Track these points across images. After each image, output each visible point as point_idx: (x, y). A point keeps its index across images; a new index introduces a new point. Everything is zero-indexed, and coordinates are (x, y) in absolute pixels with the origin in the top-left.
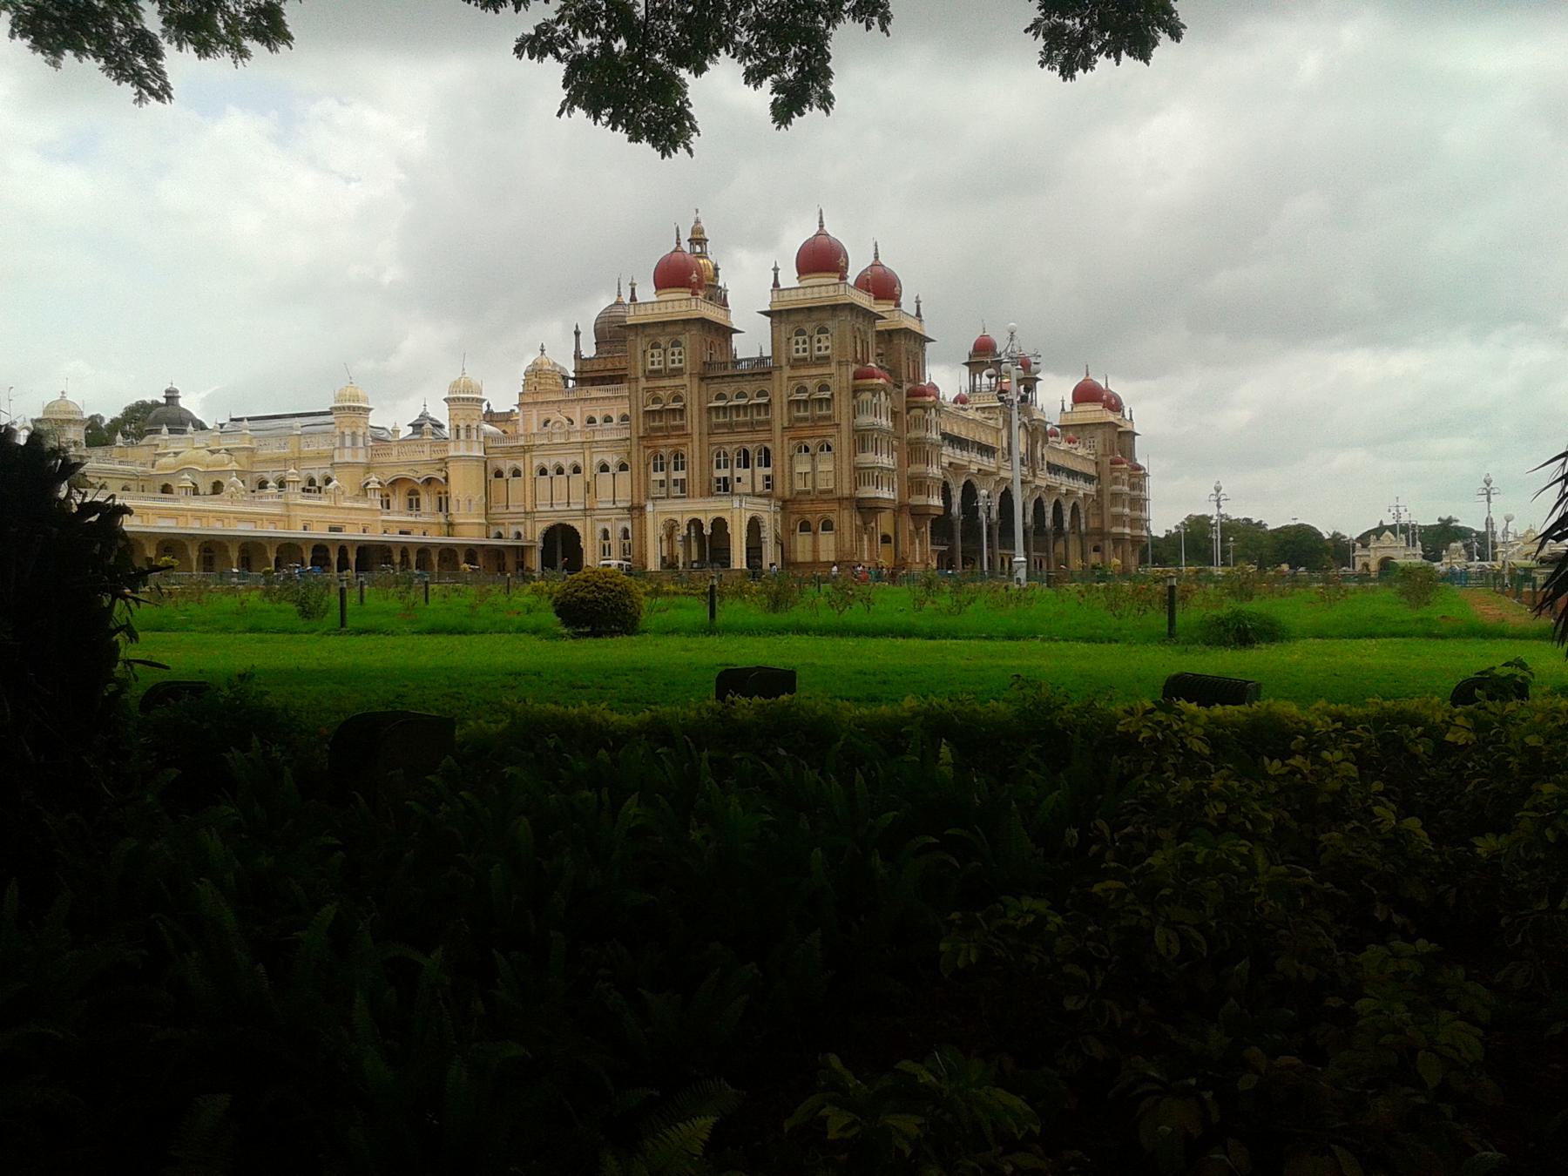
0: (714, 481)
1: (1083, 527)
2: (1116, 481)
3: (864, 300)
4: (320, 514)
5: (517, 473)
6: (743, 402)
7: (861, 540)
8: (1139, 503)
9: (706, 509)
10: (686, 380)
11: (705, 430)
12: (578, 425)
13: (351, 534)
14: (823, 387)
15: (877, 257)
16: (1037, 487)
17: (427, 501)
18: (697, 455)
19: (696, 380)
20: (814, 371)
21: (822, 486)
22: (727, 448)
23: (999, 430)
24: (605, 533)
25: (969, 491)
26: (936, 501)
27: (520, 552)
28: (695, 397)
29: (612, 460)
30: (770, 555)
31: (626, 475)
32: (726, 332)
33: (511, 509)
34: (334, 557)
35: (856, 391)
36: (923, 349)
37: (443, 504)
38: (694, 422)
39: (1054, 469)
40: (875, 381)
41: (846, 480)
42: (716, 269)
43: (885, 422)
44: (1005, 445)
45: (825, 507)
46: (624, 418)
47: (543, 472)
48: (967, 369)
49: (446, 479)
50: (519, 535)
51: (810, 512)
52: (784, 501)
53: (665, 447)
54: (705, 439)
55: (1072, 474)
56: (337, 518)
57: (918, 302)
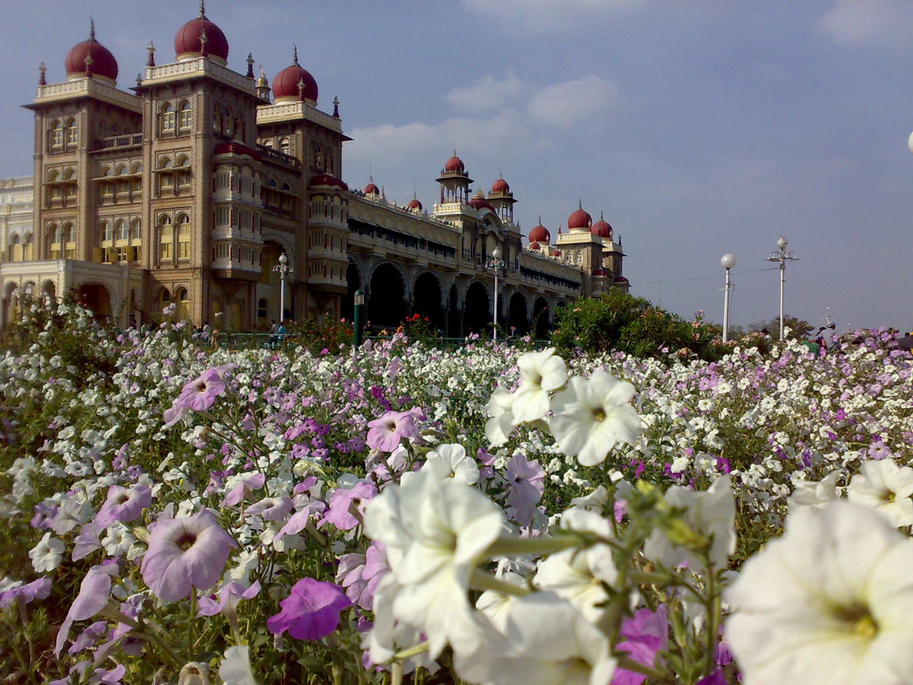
18: (83, 226)
19: (84, 156)
20: (177, 145)
22: (110, 220)
23: (458, 235)
28: (84, 170)
39: (526, 271)
41: (199, 249)
44: (467, 246)
45: (182, 276)
51: (167, 281)
53: (60, 217)
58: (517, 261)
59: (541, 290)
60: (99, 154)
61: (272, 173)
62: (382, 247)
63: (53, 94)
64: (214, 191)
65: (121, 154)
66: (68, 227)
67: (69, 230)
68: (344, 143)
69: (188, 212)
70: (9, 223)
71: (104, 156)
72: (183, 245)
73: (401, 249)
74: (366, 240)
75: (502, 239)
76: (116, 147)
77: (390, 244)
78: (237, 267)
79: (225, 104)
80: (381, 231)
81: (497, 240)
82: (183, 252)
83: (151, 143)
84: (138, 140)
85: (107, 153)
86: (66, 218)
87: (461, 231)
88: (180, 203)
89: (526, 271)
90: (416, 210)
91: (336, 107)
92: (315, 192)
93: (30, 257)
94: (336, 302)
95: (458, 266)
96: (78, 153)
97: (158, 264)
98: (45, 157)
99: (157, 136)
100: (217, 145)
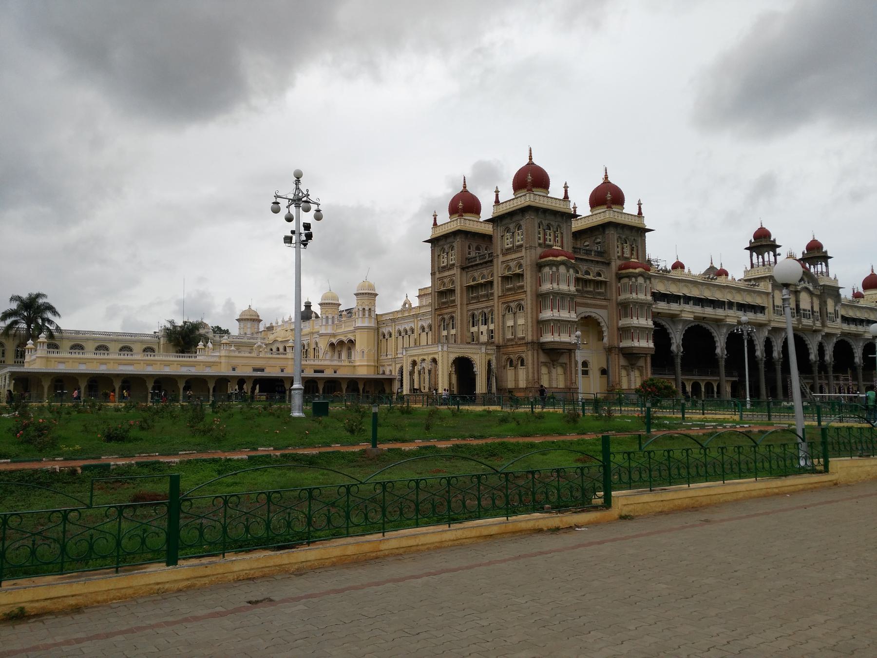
0: (469, 335)
4: (245, 361)
6: (482, 281)
11: (465, 302)
15: (606, 177)
16: (828, 336)
18: (459, 318)
20: (514, 256)
21: (520, 335)
22: (476, 312)
23: (768, 294)
29: (426, 325)
33: (389, 357)
35: (540, 267)
38: (457, 297)
39: (845, 319)
40: (551, 258)
41: (530, 329)
48: (748, 252)
52: (498, 347)
54: (465, 306)
56: (259, 363)
57: (640, 204)
60: (468, 267)
61: (584, 267)
62: (689, 312)
63: (440, 232)
65: (480, 267)
66: (452, 318)
68: (647, 234)
69: (523, 302)
71: (470, 269)
73: (709, 312)
74: (674, 307)
75: (819, 293)
77: (698, 310)
78: (557, 339)
79: (547, 222)
80: (687, 299)
81: (811, 293)
84: (491, 255)
85: (472, 266)
87: (770, 290)
88: (516, 297)
89: (845, 319)
91: (640, 209)
93: (430, 343)
94: (646, 360)
95: (770, 321)
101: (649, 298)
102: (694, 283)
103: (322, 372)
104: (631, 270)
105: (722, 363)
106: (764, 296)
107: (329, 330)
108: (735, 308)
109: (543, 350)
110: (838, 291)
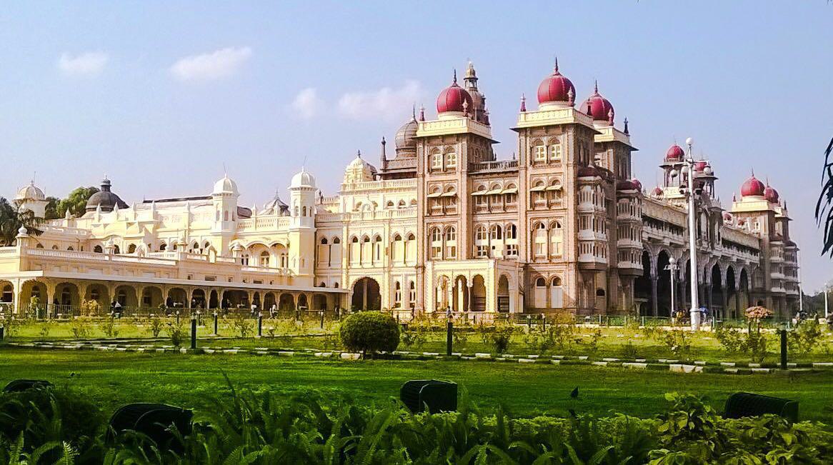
0: (475, 248)
1: (750, 287)
2: (772, 254)
3: (586, 121)
5: (337, 241)
7: (582, 292)
8: (791, 270)
9: (470, 269)
10: (458, 176)
12: (380, 208)
13: (221, 282)
14: (554, 182)
16: (715, 257)
17: (274, 261)
18: (465, 229)
19: (465, 176)
20: (549, 171)
22: (486, 225)
24: (398, 284)
25: (663, 258)
26: (638, 266)
27: (338, 297)
30: (515, 305)
31: (413, 243)
32: (487, 142)
33: (332, 266)
34: (208, 298)
36: (629, 155)
37: (284, 259)
39: (727, 243)
40: (592, 178)
42: (483, 99)
43: (602, 208)
45: (556, 268)
46: (414, 202)
47: (355, 240)
49: (288, 245)
50: (337, 285)
53: (441, 223)
55: (741, 248)
58: (719, 233)
59: (734, 259)
64: (578, 204)
67: (449, 231)
69: (561, 221)
70: (391, 225)
71: (481, 176)
72: (555, 246)
76: (489, 170)
78: (597, 261)
82: (555, 250)
83: (526, 168)
85: (484, 174)
86: (447, 222)
89: (727, 243)
90: (661, 197)
91: (626, 126)
92: (622, 196)
96: (458, 174)
97: (534, 258)
98: (427, 175)
99: (531, 163)
100: (582, 168)
101: (641, 219)
102: (651, 202)
103: (260, 282)
104: (631, 191)
105: (655, 283)
106: (682, 217)
107: (229, 230)
108: (668, 229)
109: (580, 270)
110: (721, 214)
